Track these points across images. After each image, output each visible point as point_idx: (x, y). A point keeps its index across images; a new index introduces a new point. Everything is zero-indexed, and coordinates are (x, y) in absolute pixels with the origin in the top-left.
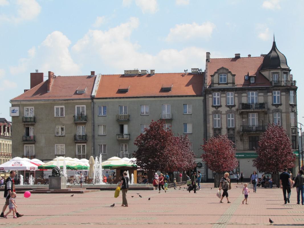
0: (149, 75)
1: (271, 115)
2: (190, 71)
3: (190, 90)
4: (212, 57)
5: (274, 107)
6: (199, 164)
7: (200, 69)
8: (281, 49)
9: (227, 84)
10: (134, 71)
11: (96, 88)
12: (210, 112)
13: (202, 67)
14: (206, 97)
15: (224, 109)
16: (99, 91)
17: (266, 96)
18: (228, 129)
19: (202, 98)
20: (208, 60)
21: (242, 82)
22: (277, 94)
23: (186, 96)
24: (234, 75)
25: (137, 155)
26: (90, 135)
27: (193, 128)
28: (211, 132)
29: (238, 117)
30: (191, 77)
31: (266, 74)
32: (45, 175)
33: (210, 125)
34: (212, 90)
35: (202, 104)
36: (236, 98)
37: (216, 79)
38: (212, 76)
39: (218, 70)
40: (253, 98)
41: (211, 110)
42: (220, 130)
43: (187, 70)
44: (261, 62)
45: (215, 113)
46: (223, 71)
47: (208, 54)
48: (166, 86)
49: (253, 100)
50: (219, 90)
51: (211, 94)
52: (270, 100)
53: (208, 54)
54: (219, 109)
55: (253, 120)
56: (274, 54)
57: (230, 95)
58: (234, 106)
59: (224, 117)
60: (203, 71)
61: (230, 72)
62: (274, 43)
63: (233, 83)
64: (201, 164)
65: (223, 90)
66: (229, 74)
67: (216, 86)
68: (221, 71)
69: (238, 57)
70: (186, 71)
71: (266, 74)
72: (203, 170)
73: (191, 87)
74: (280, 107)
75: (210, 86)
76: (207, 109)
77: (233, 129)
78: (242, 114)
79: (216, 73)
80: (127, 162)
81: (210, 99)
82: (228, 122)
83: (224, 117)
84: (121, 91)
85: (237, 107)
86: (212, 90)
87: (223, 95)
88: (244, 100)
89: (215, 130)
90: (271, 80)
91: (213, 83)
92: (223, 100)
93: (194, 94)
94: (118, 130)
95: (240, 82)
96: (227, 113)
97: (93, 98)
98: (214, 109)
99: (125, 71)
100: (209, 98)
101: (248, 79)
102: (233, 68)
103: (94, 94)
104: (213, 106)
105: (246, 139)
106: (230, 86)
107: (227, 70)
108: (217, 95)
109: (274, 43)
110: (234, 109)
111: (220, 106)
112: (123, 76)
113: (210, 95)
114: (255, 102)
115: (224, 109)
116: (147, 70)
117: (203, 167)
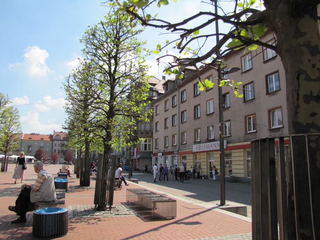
0: (38, 135)
2: (49, 134)
3: (49, 140)
4: (55, 131)
11: (23, 137)
15: (57, 145)
16: (23, 138)
18: (58, 150)
20: (54, 132)
25: (35, 156)
26: (20, 150)
27: (49, 150)
28: (53, 151)
29: (61, 147)
30: (49, 136)
33: (53, 149)
34: (54, 140)
35: (52, 143)
38: (55, 136)
41: (54, 145)
42: (56, 150)
45: (55, 146)
46: (58, 135)
47: (54, 130)
48: (42, 138)
53: (54, 130)
55: (65, 149)
59: (57, 147)
63: (60, 138)
65: (58, 140)
67: (56, 139)
73: (49, 139)
77: (59, 150)
80: (32, 157)
82: (58, 148)
83: (57, 147)
84: (30, 138)
86: (54, 140)
89: (54, 150)
91: (55, 138)
94: (28, 149)
95: (62, 139)
96: (58, 146)
97: (22, 140)
101: (64, 138)
103: (22, 139)
105: (62, 153)
106: (59, 139)
108: (56, 141)
112: (31, 134)
115: (57, 145)
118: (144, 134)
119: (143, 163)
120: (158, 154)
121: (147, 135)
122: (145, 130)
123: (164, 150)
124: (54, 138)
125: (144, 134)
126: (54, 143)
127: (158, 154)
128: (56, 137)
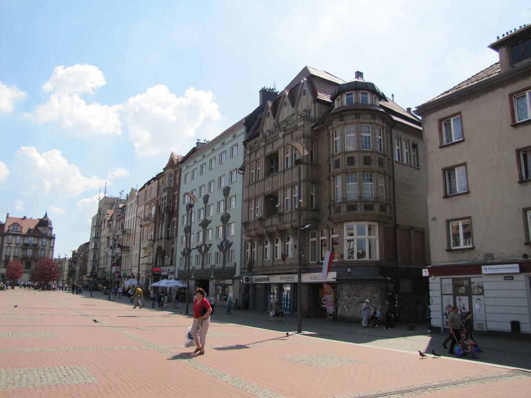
1: (40, 251)
4: (10, 216)
5: (42, 247)
8: (49, 217)
9: (17, 231)
12: (5, 246)
15: (13, 245)
17: (38, 241)
18: (14, 256)
20: (7, 217)
21: (26, 231)
22: (44, 240)
24: (22, 227)
29: (21, 250)
31: (40, 229)
34: (8, 234)
36: (22, 240)
37: (11, 228)
38: (9, 226)
40: (31, 241)
41: (5, 245)
42: (9, 256)
44: (38, 222)
45: (7, 247)
46: (16, 224)
47: (8, 214)
49: (31, 242)
50: (12, 234)
52: (40, 242)
53: (8, 214)
54: (11, 245)
55: (30, 253)
56: (45, 219)
57: (18, 238)
58: (20, 244)
59: (13, 250)
60: (4, 223)
61: (20, 226)
62: (46, 213)
63: (21, 232)
65: (14, 235)
67: (11, 232)
69: (25, 218)
71: (40, 229)
74: (45, 247)
75: (7, 232)
77: (17, 257)
78: (23, 249)
81: (6, 239)
82: (15, 252)
83: (13, 250)
85: (21, 245)
86: (8, 234)
87: (14, 237)
88: (26, 242)
89: (6, 256)
90: (42, 232)
91: (9, 230)
92: (14, 241)
95: (25, 231)
96: (15, 247)
98: (7, 245)
101: (30, 230)
102: (22, 223)
105: (24, 262)
107: (18, 224)
108: (10, 237)
109: (46, 213)
110: (19, 246)
111: (11, 243)
114: (32, 243)
115: (13, 245)
118: (360, 210)
119: (355, 297)
120: (483, 267)
121: (368, 212)
122: (344, 200)
123: (527, 253)
124: (6, 229)
125: (360, 210)
126: (6, 241)
127: (483, 267)
128: (11, 227)
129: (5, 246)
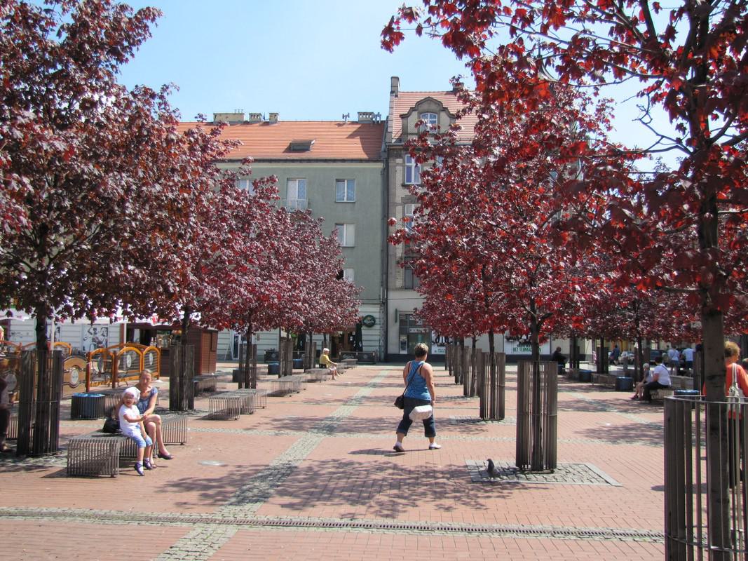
0: (266, 124)
3: (355, 149)
6: (369, 318)
7: (376, 113)
10: (235, 114)
12: (398, 200)
13: (381, 107)
14: (390, 164)
19: (380, 166)
20: (394, 92)
23: (343, 161)
27: (358, 234)
32: (13, 334)
35: (382, 174)
38: (402, 116)
39: (419, 103)
43: (348, 116)
51: (400, 157)
60: (383, 118)
61: (445, 109)
64: (373, 319)
66: (443, 115)
68: (425, 106)
70: (346, 116)
72: (378, 333)
73: (357, 140)
75: (399, 140)
76: (391, 191)
79: (413, 109)
81: (399, 169)
91: (405, 132)
93: (365, 156)
98: (406, 192)
99: (215, 115)
100: (395, 166)
104: (404, 186)
107: (440, 103)
113: (399, 161)
116: (263, 115)
117: (377, 327)
124: (395, 129)
128: (414, 119)
129: (398, 200)
